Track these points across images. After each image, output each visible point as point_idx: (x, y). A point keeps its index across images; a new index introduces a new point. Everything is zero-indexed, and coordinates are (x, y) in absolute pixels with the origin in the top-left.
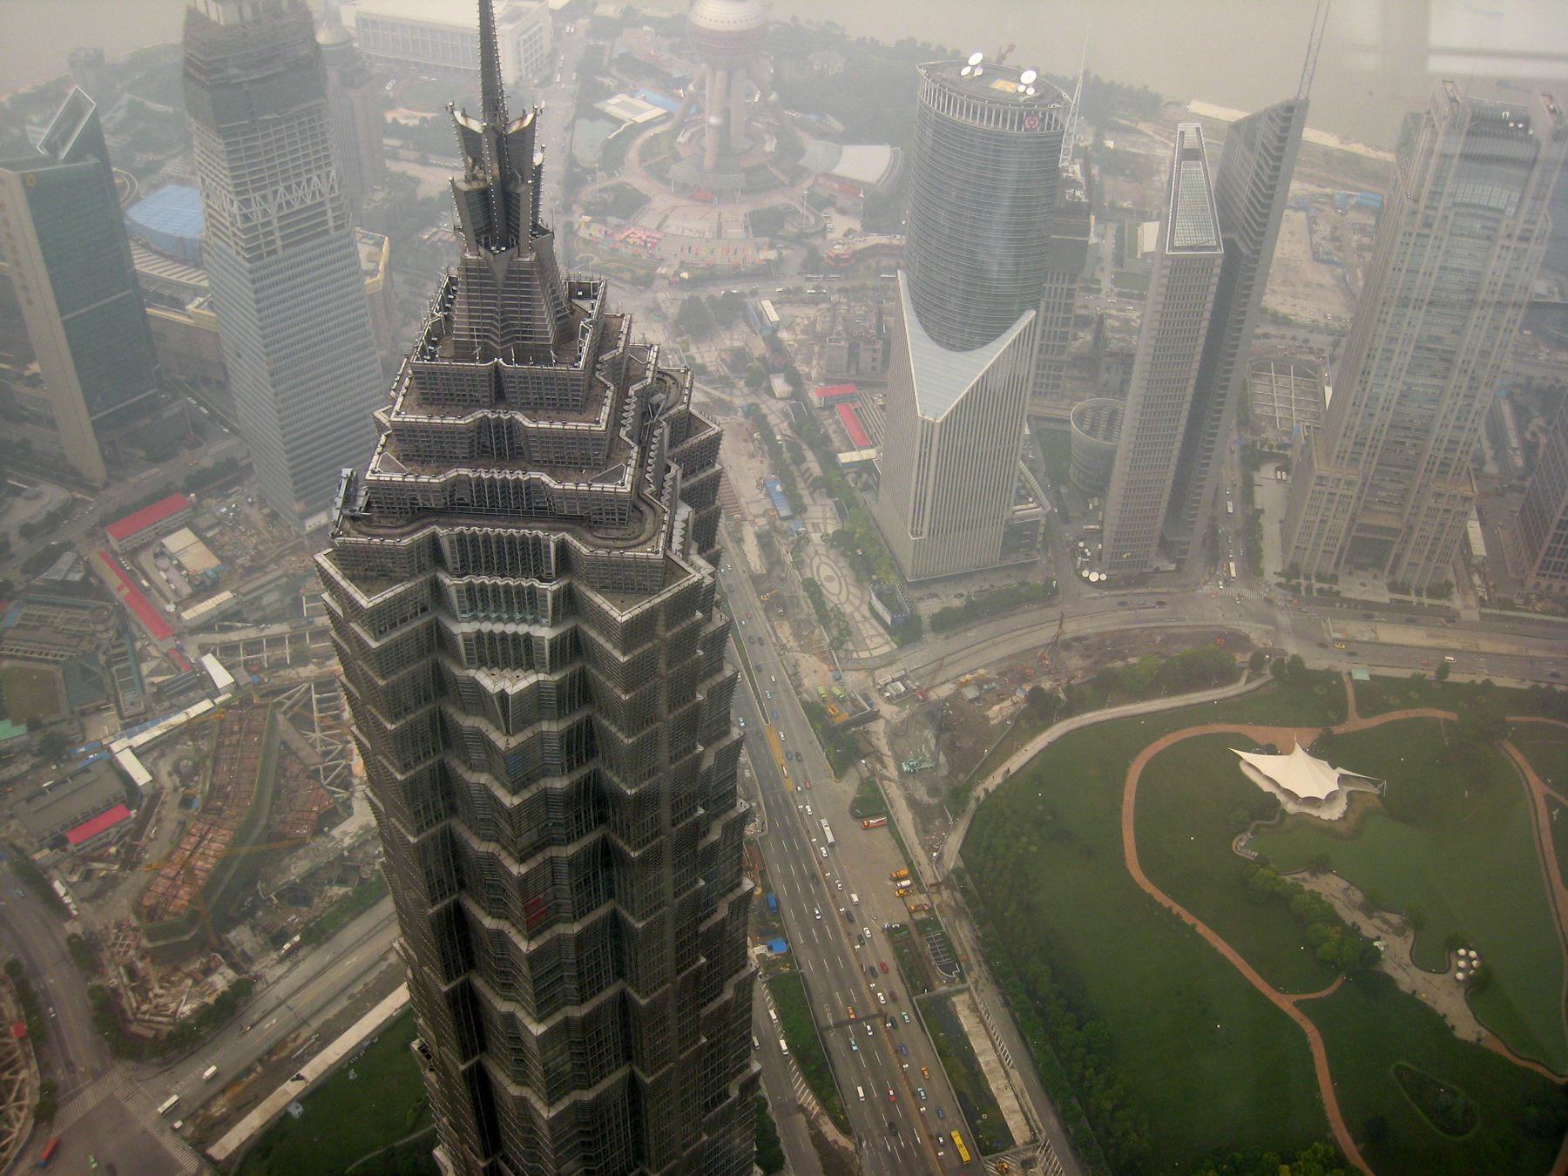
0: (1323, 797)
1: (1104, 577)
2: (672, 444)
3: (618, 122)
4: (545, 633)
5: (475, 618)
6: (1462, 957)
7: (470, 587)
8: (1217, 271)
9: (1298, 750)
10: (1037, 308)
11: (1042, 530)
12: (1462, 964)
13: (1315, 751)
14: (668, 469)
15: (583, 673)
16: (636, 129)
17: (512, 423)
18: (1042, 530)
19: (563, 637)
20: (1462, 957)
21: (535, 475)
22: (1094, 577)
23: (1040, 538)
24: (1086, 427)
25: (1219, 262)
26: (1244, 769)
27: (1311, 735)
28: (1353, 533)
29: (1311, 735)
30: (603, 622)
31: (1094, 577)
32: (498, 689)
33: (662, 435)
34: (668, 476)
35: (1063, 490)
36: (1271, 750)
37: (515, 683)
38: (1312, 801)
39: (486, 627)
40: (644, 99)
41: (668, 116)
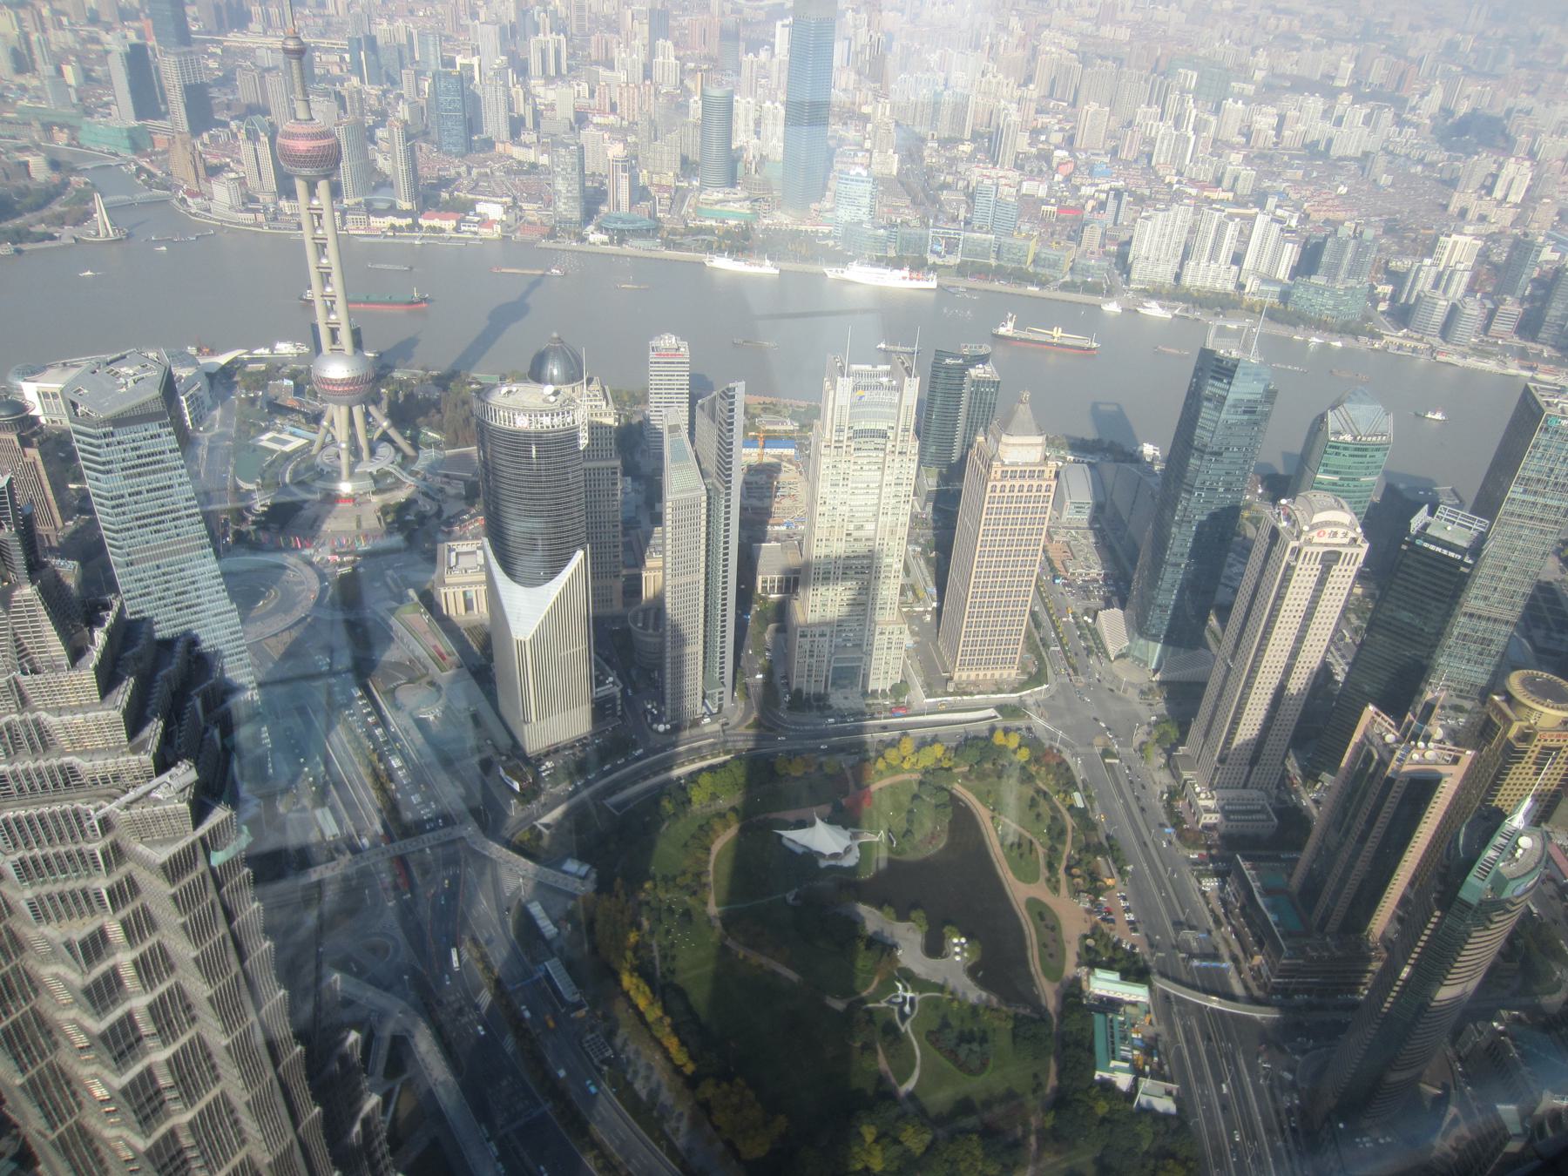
0: (840, 850)
1: (668, 726)
2: (207, 708)
3: (273, 451)
4: (102, 883)
5: (32, 885)
6: (956, 945)
7: (22, 861)
8: (704, 505)
9: (818, 821)
10: (584, 549)
11: (619, 702)
12: (957, 949)
13: (830, 821)
14: (206, 730)
15: (145, 909)
16: (288, 457)
17: (37, 723)
18: (619, 702)
19: (119, 885)
20: (956, 945)
21: (67, 759)
22: (661, 728)
23: (619, 708)
24: (640, 625)
25: (704, 498)
26: (785, 841)
27: (826, 809)
28: (833, 665)
29: (826, 809)
30: (145, 864)
31: (661, 728)
32: (64, 939)
33: (194, 706)
34: (208, 735)
35: (634, 673)
36: (802, 824)
37: (80, 929)
38: (835, 856)
39: (44, 890)
40: (292, 434)
41: (311, 443)
